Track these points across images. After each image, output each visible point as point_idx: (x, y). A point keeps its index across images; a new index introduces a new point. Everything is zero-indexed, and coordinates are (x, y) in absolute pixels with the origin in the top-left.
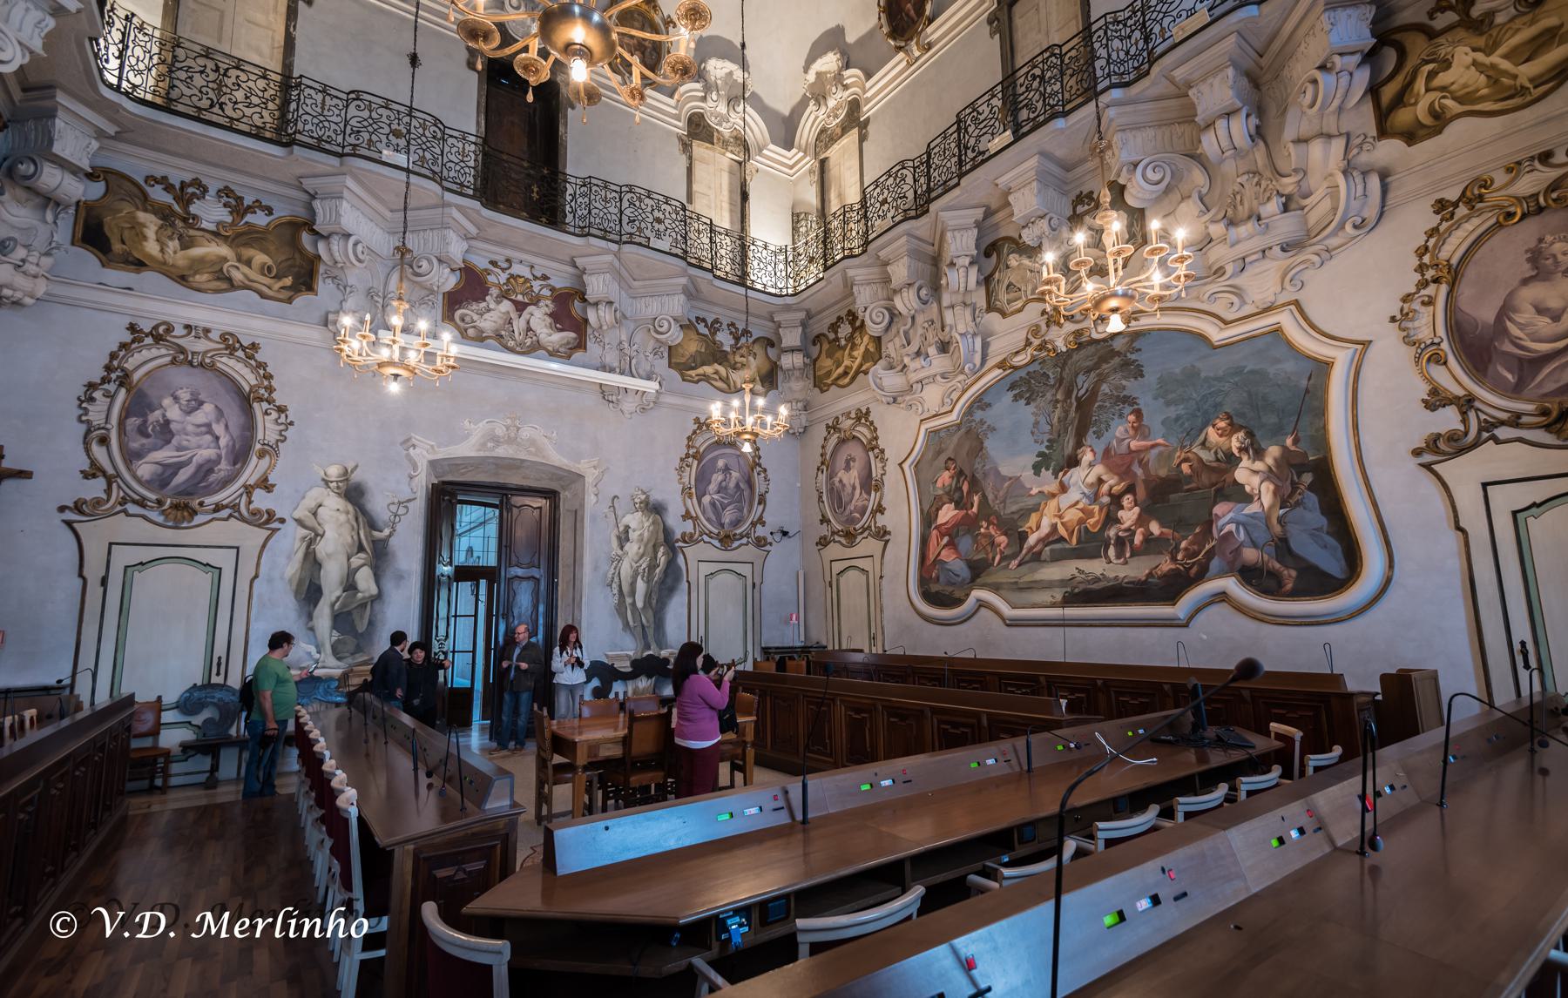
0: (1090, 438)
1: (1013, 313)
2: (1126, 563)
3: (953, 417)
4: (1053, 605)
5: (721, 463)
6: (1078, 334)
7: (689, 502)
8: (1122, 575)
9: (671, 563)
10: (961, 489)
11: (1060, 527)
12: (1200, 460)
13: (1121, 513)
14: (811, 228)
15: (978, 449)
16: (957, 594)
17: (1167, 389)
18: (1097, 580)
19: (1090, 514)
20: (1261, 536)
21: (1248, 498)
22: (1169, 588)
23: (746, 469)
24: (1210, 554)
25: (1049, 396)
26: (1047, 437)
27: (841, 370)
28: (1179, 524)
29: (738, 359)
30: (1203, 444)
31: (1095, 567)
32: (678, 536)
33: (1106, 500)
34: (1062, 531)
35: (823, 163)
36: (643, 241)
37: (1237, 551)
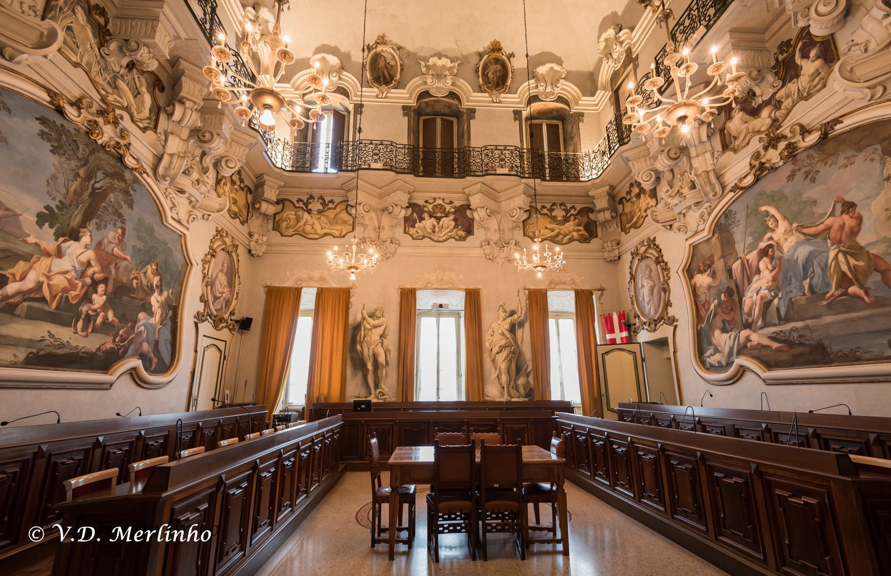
2: (87, 336)
8: (81, 346)
12: (141, 282)
13: (94, 296)
17: (139, 224)
18: (62, 346)
19: (73, 287)
21: (151, 314)
22: (104, 361)
26: (59, 197)
28: (122, 318)
30: (145, 273)
33: (88, 281)
37: (141, 343)
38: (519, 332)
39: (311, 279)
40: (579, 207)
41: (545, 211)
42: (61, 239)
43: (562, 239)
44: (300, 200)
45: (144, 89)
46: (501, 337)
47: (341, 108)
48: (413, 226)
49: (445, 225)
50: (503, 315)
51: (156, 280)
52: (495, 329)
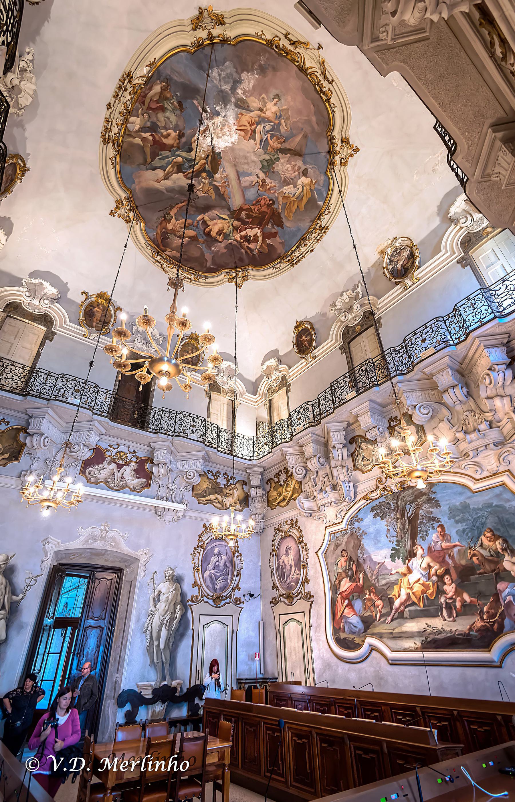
0: (419, 541)
1: (367, 471)
3: (343, 525)
4: (416, 650)
5: (216, 551)
6: (402, 483)
7: (197, 574)
8: (454, 629)
9: (184, 616)
11: (411, 594)
13: (445, 587)
14: (265, 429)
15: (359, 545)
16: (357, 640)
17: (453, 512)
18: (440, 632)
19: (427, 587)
23: (230, 554)
26: (395, 539)
27: (281, 498)
29: (228, 491)
32: (189, 598)
33: (435, 578)
35: (270, 401)
36: (185, 435)
42: (407, 561)
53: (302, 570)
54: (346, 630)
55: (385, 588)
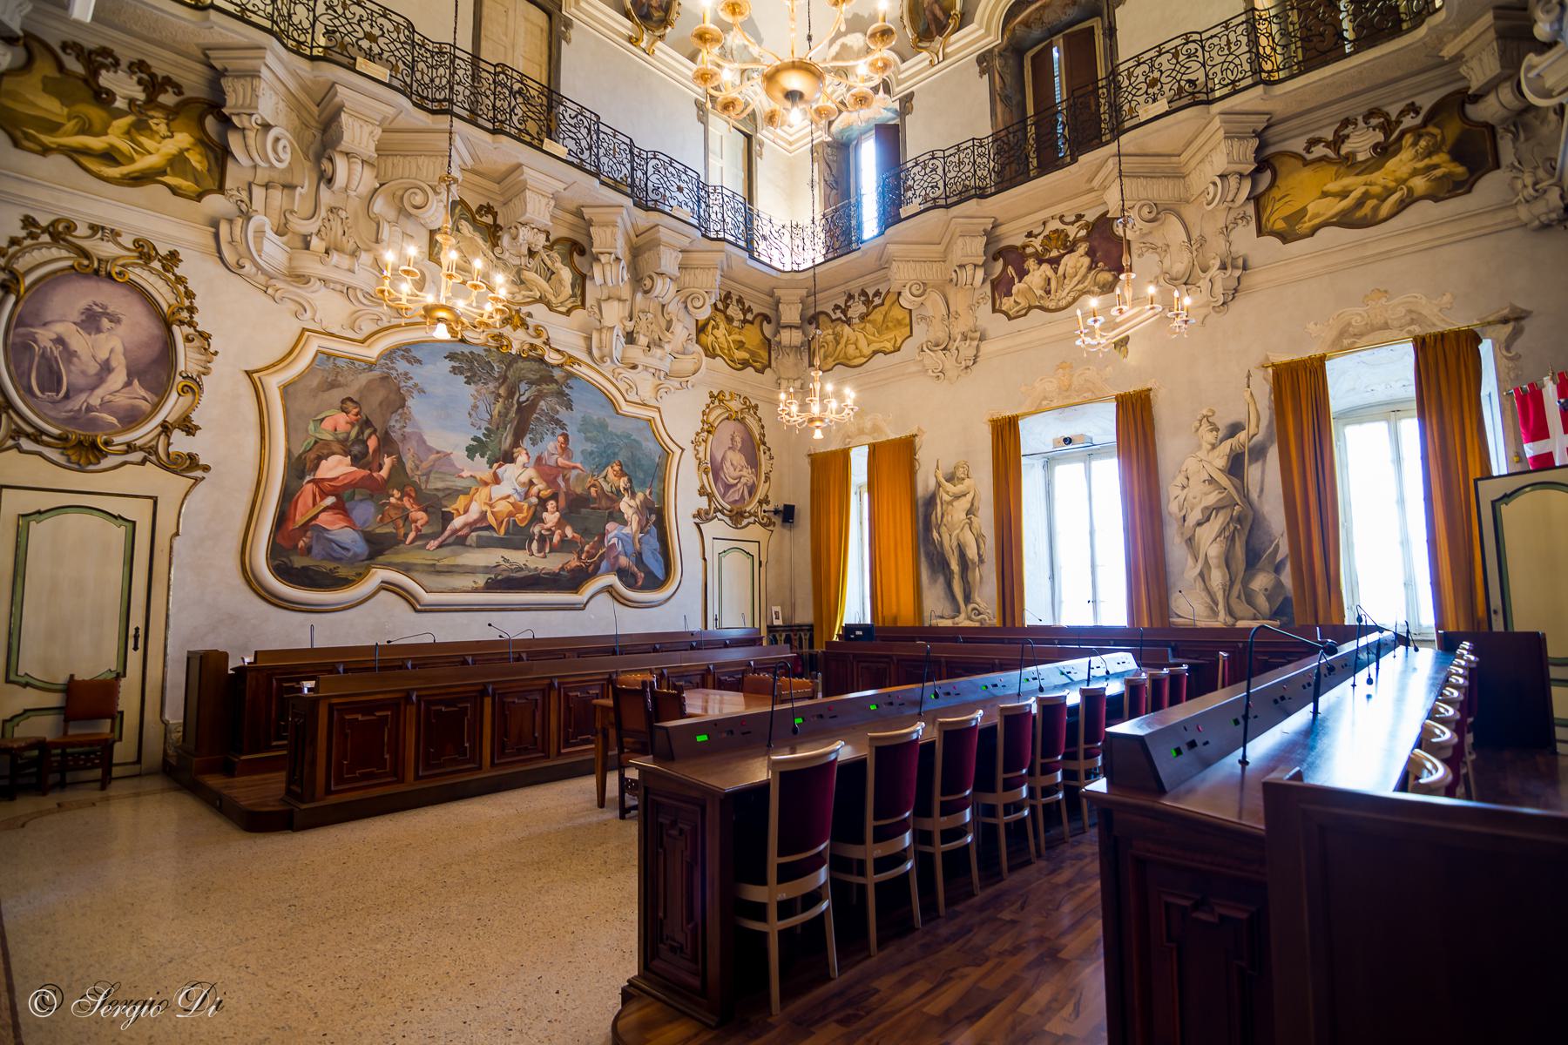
0: (526, 442)
3: (373, 352)
4: (475, 590)
6: (533, 347)
10: (365, 442)
15: (397, 403)
16: (343, 572)
17: (586, 425)
18: (520, 569)
19: (518, 509)
20: (630, 550)
21: (625, 523)
22: (573, 580)
24: (602, 558)
25: (491, 386)
28: (585, 532)
31: (519, 558)
33: (534, 500)
34: (491, 519)
37: (616, 558)
38: (1253, 472)
39: (861, 432)
40: (1426, 102)
41: (1319, 151)
43: (1376, 209)
44: (837, 307)
45: (559, 265)
46: (1207, 487)
47: (890, 115)
48: (1009, 294)
49: (1070, 271)
50: (1210, 437)
51: (623, 482)
52: (1191, 468)
53: (174, 395)
54: (315, 550)
55: (440, 494)
